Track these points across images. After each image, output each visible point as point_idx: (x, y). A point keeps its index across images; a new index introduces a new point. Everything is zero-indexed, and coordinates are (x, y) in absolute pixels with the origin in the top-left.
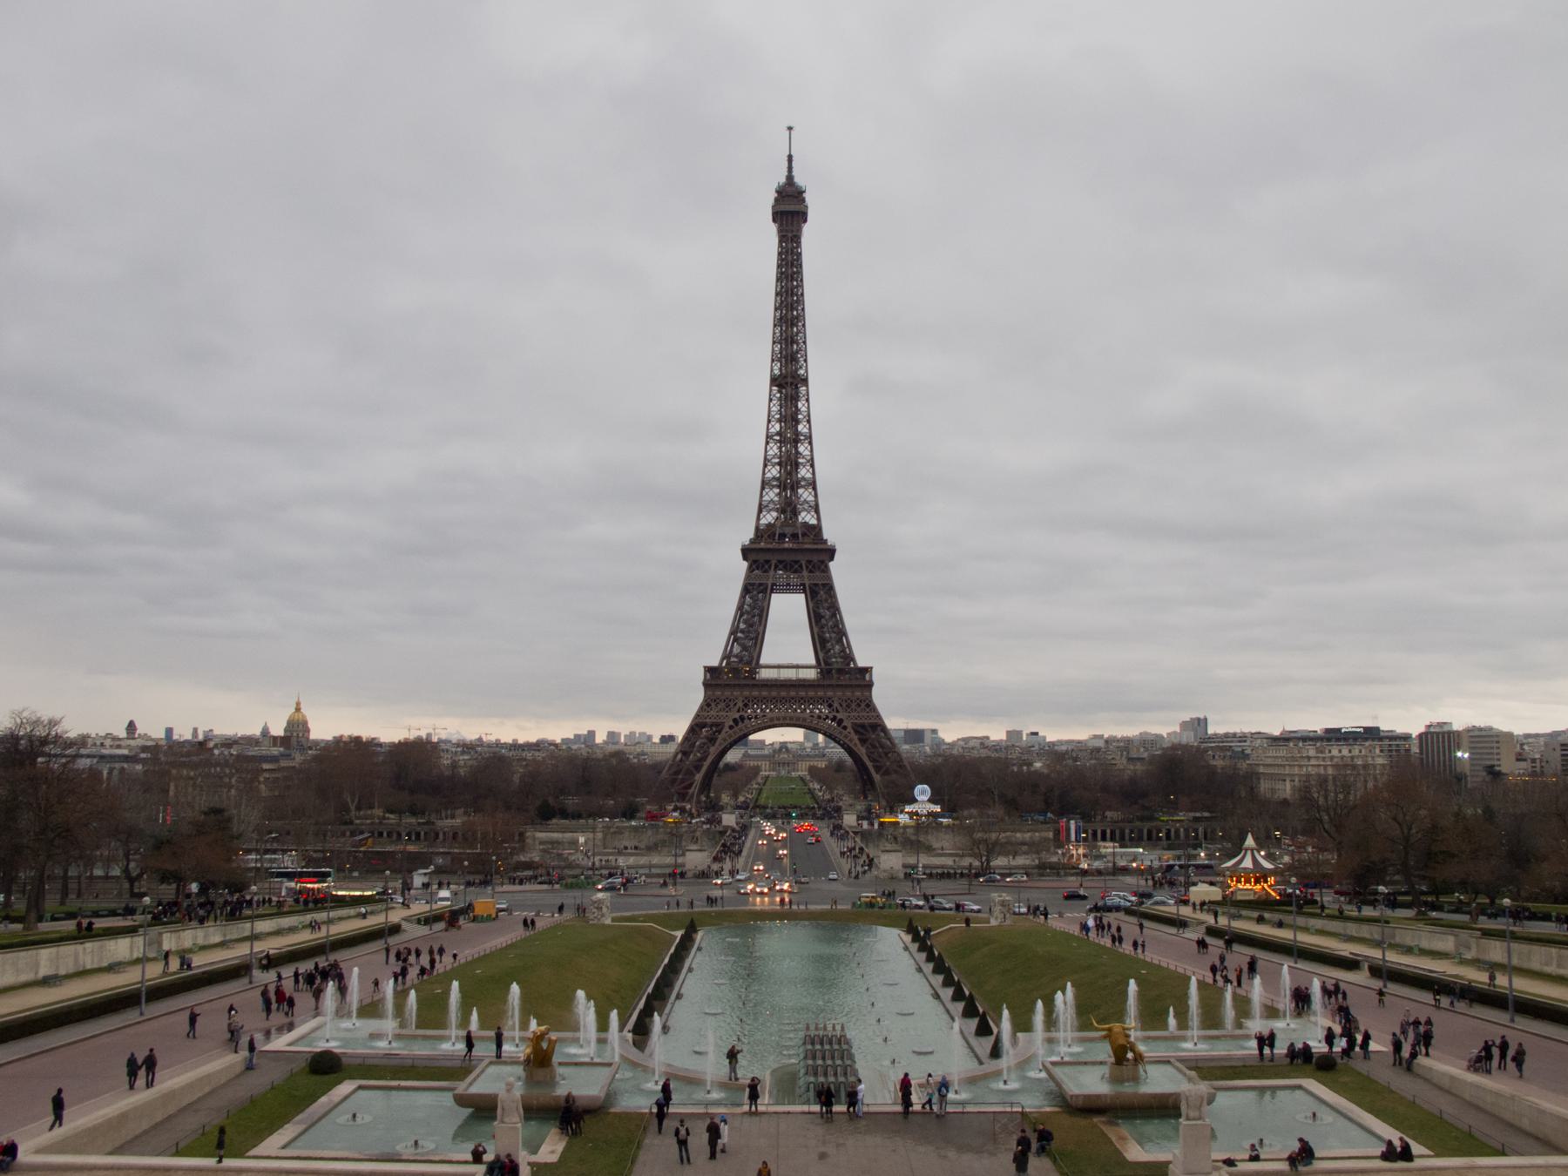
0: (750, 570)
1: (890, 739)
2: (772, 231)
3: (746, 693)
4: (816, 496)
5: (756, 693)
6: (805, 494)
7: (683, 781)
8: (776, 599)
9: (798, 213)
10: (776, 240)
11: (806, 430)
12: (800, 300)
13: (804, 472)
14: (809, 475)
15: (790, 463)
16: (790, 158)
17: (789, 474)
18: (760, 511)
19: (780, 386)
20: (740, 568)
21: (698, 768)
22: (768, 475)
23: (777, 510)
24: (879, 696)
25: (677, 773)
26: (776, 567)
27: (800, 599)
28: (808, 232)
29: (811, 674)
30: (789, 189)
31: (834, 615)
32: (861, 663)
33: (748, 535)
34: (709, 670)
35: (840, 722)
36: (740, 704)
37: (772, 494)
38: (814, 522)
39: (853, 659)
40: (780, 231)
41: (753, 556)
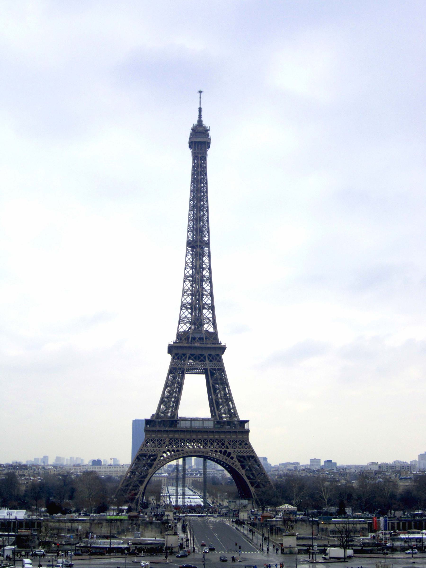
0: (173, 358)
1: (258, 465)
3: (171, 436)
4: (214, 314)
5: (177, 436)
6: (207, 313)
7: (133, 490)
9: (204, 143)
10: (191, 159)
13: (207, 300)
14: (209, 302)
16: (200, 110)
17: (198, 300)
19: (193, 247)
20: (167, 360)
21: (141, 482)
22: (185, 302)
25: (127, 486)
26: (190, 358)
30: (201, 129)
31: (224, 389)
33: (172, 339)
34: (147, 422)
35: (230, 454)
36: (167, 443)
37: (187, 313)
38: (212, 330)
41: (175, 351)
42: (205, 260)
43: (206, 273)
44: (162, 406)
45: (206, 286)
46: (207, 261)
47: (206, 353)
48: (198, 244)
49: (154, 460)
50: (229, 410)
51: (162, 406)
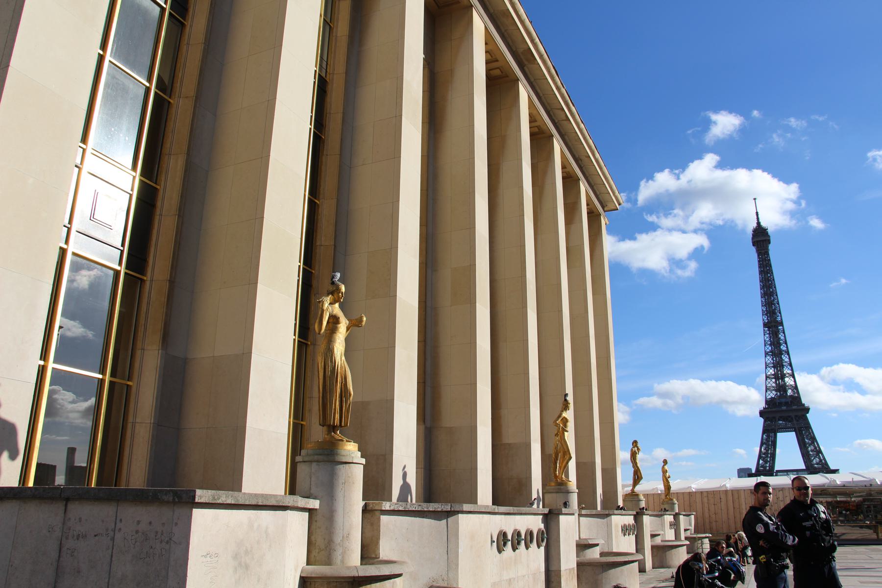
2: (754, 249)
6: (789, 381)
8: (780, 436)
10: (756, 255)
11: (784, 349)
15: (778, 365)
16: (757, 213)
23: (776, 391)
27: (793, 435)
28: (772, 248)
33: (762, 405)
37: (772, 383)
40: (757, 251)
42: (781, 336)
43: (783, 348)
44: (761, 462)
45: (785, 358)
46: (782, 338)
47: (792, 414)
48: (773, 324)
50: (821, 461)
51: (761, 462)
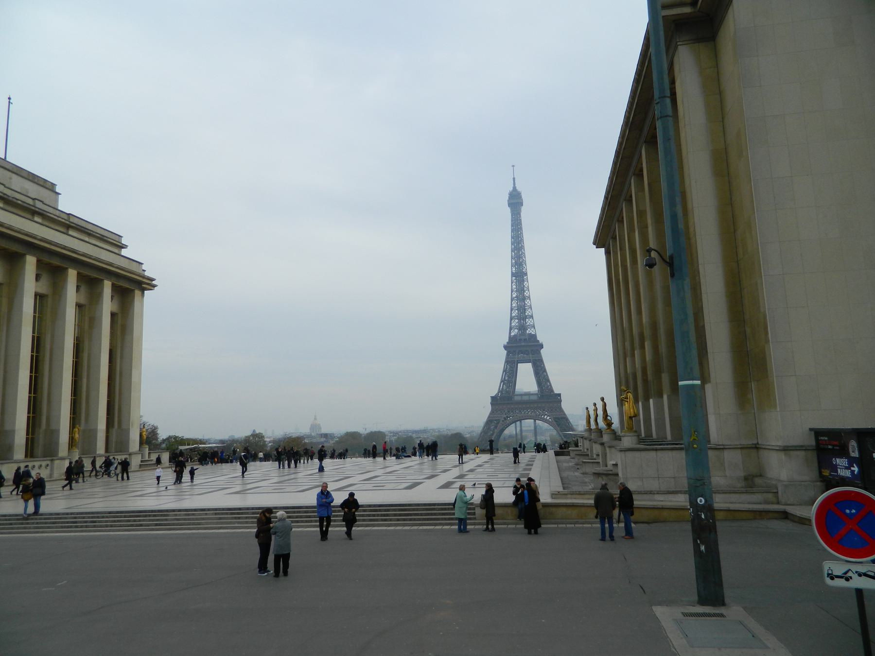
0: (508, 355)
2: (509, 210)
6: (529, 322)
12: (522, 240)
16: (514, 179)
18: (511, 329)
24: (564, 405)
27: (529, 366)
29: (535, 398)
32: (556, 391)
33: (506, 340)
34: (492, 397)
37: (515, 323)
39: (552, 391)
45: (527, 302)
49: (498, 423)
